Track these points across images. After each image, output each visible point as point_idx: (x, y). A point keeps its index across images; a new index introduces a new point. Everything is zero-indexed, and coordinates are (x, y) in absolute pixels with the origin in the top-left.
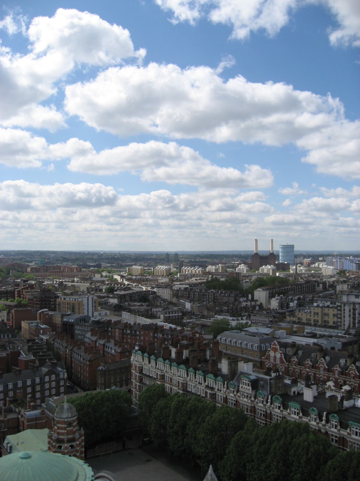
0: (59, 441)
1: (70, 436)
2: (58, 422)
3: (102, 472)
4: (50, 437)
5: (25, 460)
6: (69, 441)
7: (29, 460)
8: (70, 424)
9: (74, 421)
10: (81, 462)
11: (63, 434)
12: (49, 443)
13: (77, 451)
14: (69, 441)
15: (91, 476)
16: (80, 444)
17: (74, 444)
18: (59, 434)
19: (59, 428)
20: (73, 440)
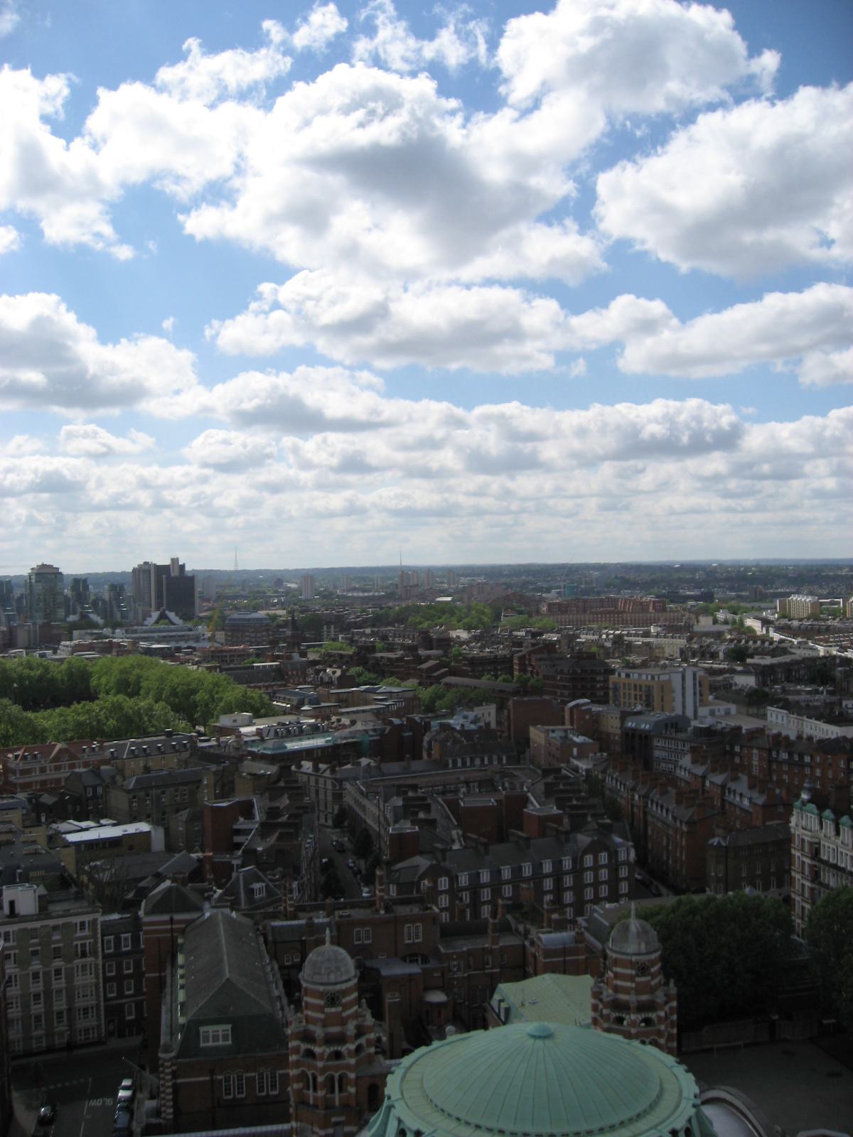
0: (617, 1005)
1: (644, 998)
2: (616, 962)
3: (719, 1089)
4: (597, 994)
5: (539, 1043)
6: (642, 1007)
7: (548, 1042)
8: (643, 969)
9: (653, 963)
10: (670, 1060)
11: (626, 991)
12: (595, 1008)
13: (660, 1033)
14: (642, 1007)
15: (692, 1097)
16: (667, 1016)
17: (653, 1016)
18: (617, 989)
19: (617, 976)
20: (651, 1006)
